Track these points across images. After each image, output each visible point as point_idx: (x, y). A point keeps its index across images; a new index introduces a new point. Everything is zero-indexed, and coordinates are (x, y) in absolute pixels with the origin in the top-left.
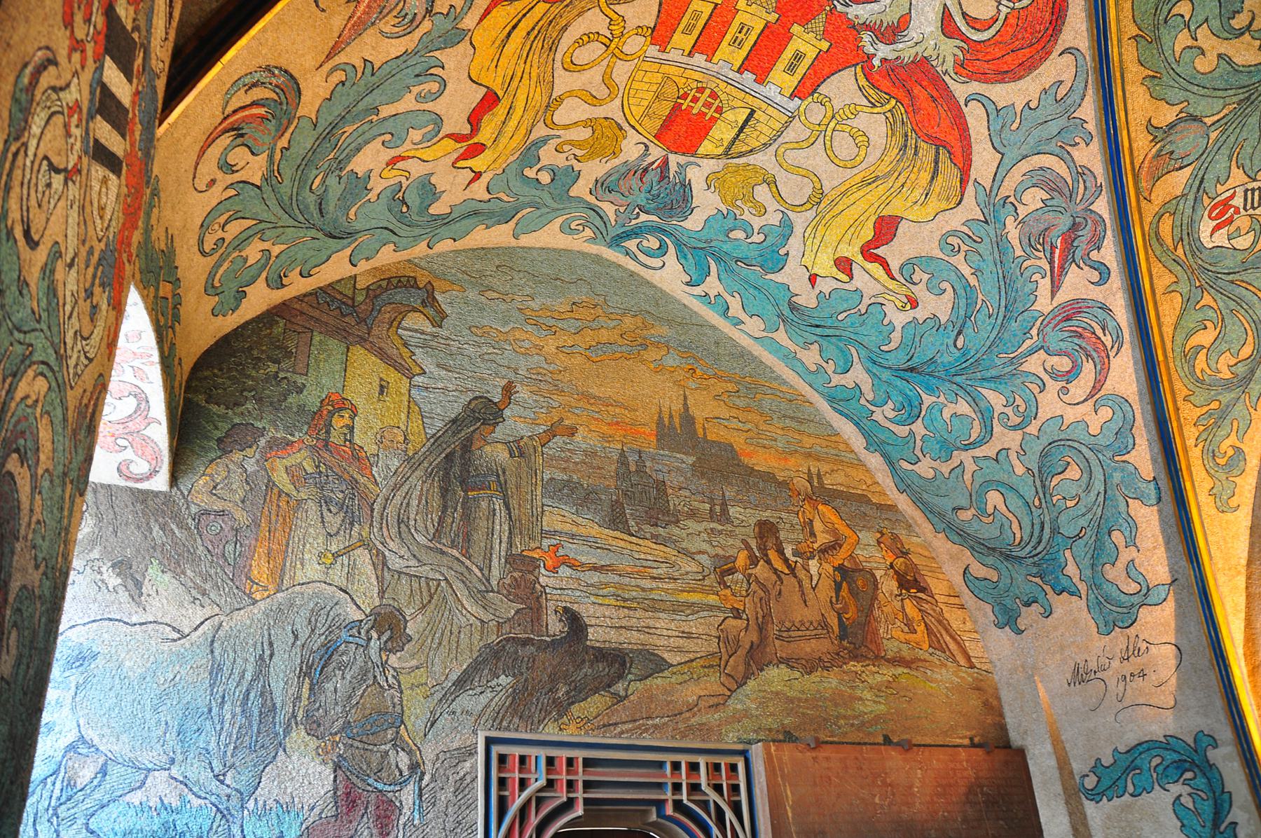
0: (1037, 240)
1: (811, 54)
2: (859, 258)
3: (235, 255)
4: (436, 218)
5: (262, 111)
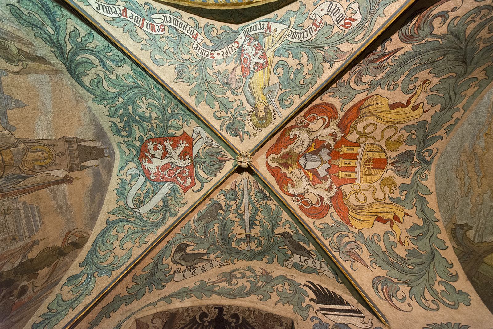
0: (381, 68)
1: (347, 147)
2: (411, 106)
3: (439, 295)
4: (424, 222)
5: (385, 288)
